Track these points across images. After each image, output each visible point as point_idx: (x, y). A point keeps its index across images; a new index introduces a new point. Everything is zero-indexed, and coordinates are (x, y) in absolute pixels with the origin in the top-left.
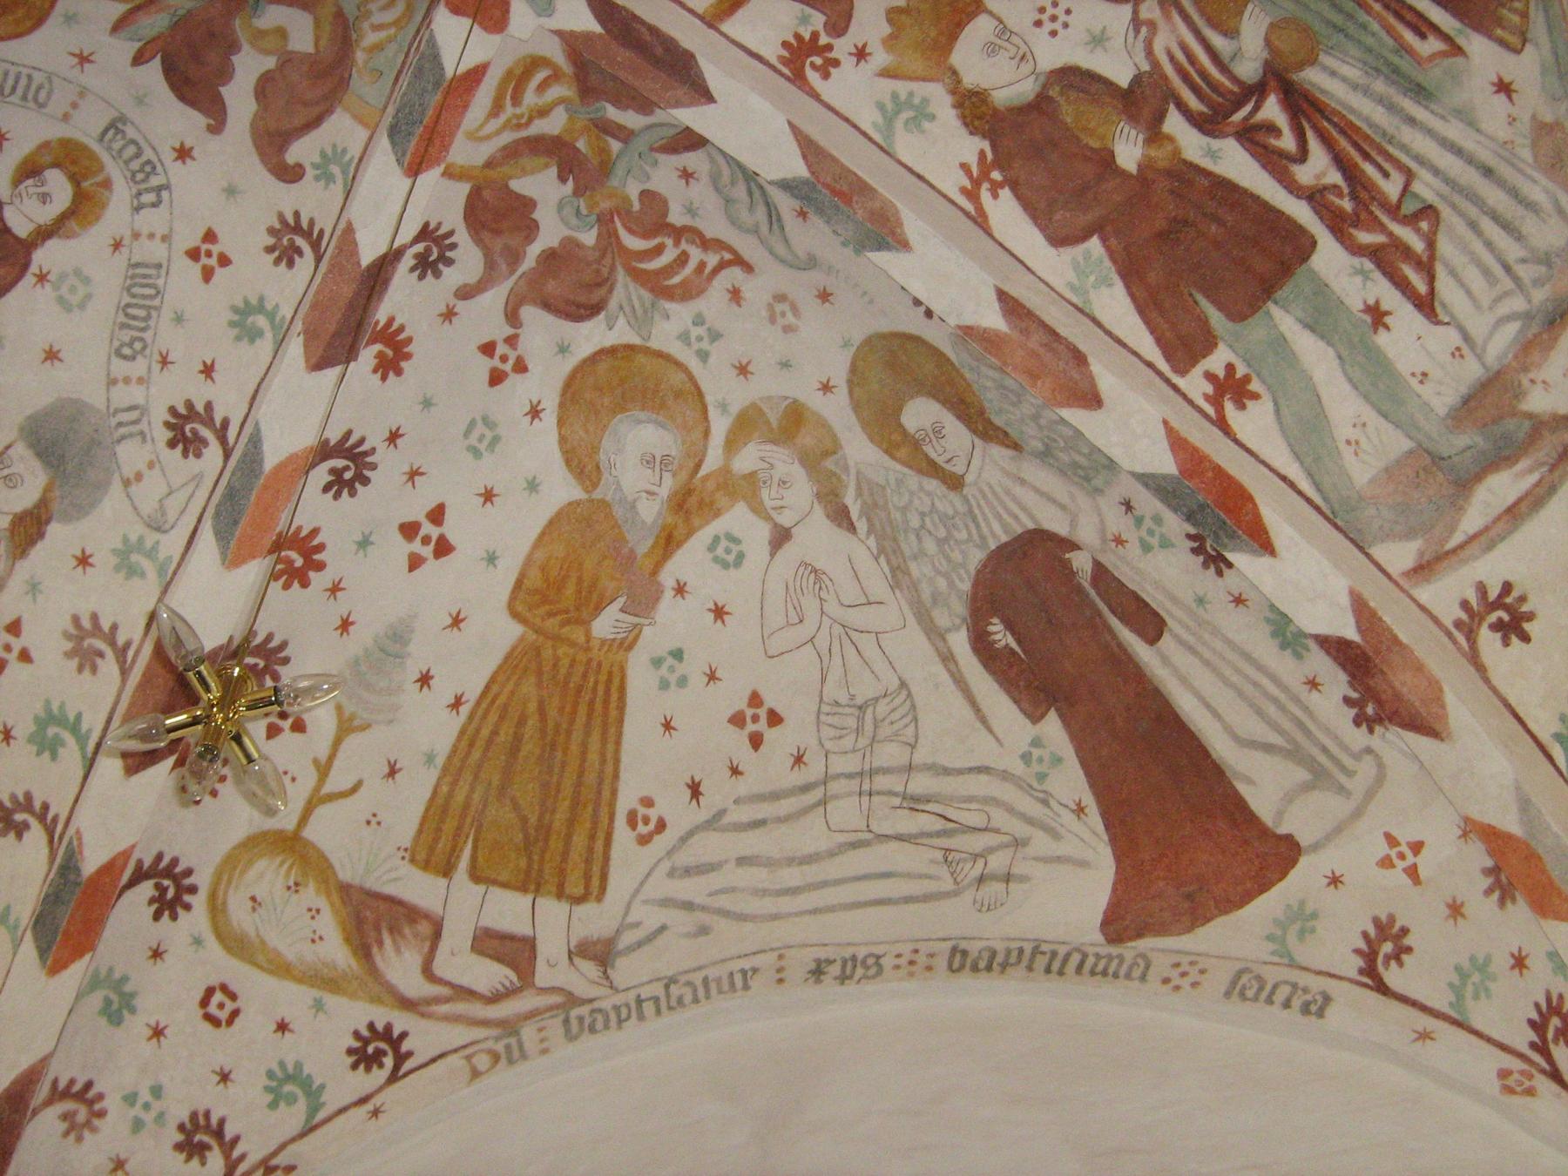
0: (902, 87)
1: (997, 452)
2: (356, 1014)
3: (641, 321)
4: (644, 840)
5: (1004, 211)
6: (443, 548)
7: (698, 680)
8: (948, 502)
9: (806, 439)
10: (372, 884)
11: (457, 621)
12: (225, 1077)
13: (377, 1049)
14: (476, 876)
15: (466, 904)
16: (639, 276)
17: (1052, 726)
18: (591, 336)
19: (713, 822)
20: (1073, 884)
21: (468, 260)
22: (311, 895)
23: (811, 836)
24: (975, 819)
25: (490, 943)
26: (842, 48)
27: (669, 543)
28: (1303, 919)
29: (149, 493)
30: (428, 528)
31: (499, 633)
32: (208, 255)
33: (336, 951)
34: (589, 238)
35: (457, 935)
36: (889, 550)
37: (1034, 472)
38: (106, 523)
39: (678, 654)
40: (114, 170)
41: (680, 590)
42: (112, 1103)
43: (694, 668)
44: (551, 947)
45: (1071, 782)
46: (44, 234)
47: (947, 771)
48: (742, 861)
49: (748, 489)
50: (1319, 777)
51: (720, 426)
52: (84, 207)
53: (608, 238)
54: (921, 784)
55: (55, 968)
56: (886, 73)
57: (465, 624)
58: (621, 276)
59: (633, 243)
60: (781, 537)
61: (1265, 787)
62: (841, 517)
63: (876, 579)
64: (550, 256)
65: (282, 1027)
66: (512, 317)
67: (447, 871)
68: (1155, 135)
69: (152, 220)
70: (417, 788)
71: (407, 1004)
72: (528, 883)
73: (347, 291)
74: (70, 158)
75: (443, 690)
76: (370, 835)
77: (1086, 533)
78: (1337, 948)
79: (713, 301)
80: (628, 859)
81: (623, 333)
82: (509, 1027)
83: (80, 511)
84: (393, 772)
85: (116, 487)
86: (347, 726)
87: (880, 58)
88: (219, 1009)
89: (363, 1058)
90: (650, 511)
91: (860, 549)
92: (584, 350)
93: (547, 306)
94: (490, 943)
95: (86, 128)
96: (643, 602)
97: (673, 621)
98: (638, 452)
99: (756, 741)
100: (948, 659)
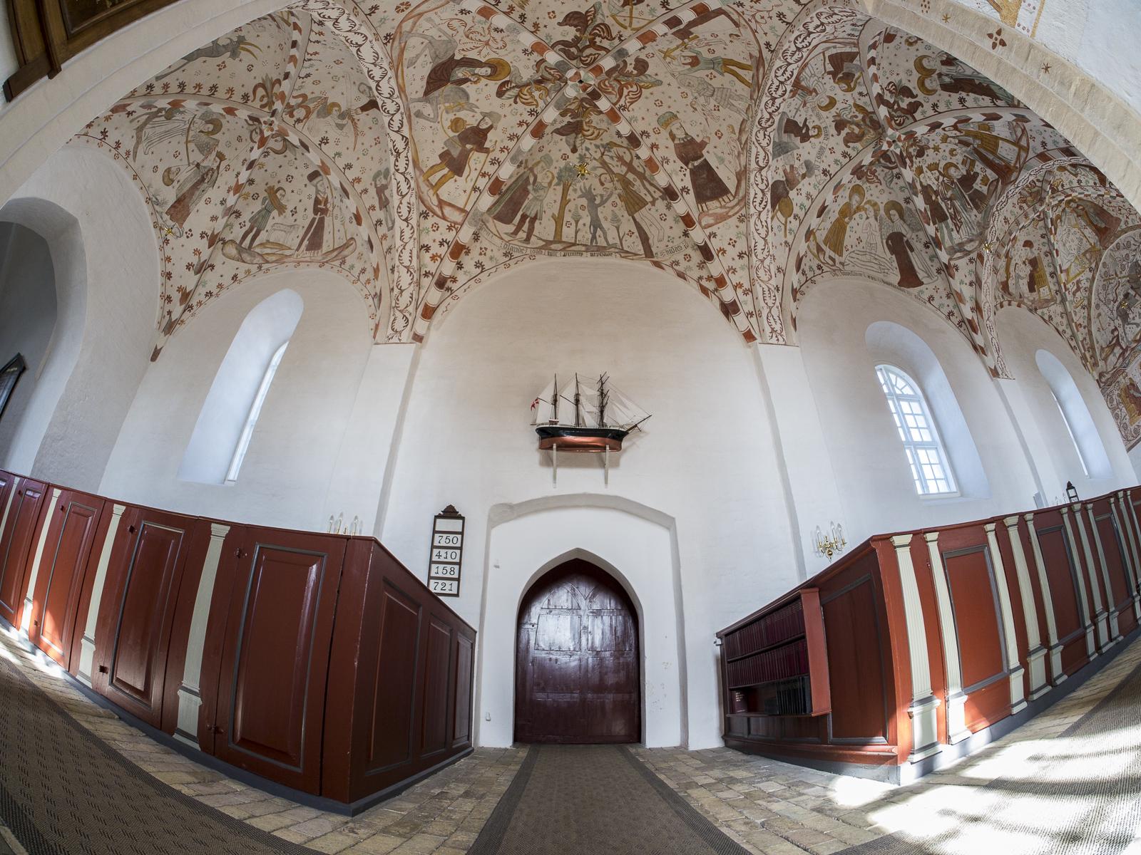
1: (902, 222)
8: (891, 224)
9: (876, 208)
13: (819, 267)
15: (829, 252)
17: (894, 256)
18: (858, 182)
20: (895, 277)
23: (864, 258)
25: (830, 257)
27: (855, 213)
28: (922, 292)
29: (819, 178)
31: (837, 215)
32: (832, 150)
36: (881, 225)
37: (905, 226)
38: (813, 180)
45: (895, 264)
46: (813, 136)
49: (865, 210)
50: (929, 276)
52: (818, 136)
60: (868, 218)
61: (921, 275)
62: (876, 219)
63: (878, 229)
70: (826, 232)
77: (908, 236)
78: (926, 297)
79: (873, 186)
80: (845, 253)
81: (861, 184)
83: (810, 177)
85: (814, 176)
90: (854, 207)
91: (877, 224)
94: (830, 257)
96: (850, 219)
97: (853, 223)
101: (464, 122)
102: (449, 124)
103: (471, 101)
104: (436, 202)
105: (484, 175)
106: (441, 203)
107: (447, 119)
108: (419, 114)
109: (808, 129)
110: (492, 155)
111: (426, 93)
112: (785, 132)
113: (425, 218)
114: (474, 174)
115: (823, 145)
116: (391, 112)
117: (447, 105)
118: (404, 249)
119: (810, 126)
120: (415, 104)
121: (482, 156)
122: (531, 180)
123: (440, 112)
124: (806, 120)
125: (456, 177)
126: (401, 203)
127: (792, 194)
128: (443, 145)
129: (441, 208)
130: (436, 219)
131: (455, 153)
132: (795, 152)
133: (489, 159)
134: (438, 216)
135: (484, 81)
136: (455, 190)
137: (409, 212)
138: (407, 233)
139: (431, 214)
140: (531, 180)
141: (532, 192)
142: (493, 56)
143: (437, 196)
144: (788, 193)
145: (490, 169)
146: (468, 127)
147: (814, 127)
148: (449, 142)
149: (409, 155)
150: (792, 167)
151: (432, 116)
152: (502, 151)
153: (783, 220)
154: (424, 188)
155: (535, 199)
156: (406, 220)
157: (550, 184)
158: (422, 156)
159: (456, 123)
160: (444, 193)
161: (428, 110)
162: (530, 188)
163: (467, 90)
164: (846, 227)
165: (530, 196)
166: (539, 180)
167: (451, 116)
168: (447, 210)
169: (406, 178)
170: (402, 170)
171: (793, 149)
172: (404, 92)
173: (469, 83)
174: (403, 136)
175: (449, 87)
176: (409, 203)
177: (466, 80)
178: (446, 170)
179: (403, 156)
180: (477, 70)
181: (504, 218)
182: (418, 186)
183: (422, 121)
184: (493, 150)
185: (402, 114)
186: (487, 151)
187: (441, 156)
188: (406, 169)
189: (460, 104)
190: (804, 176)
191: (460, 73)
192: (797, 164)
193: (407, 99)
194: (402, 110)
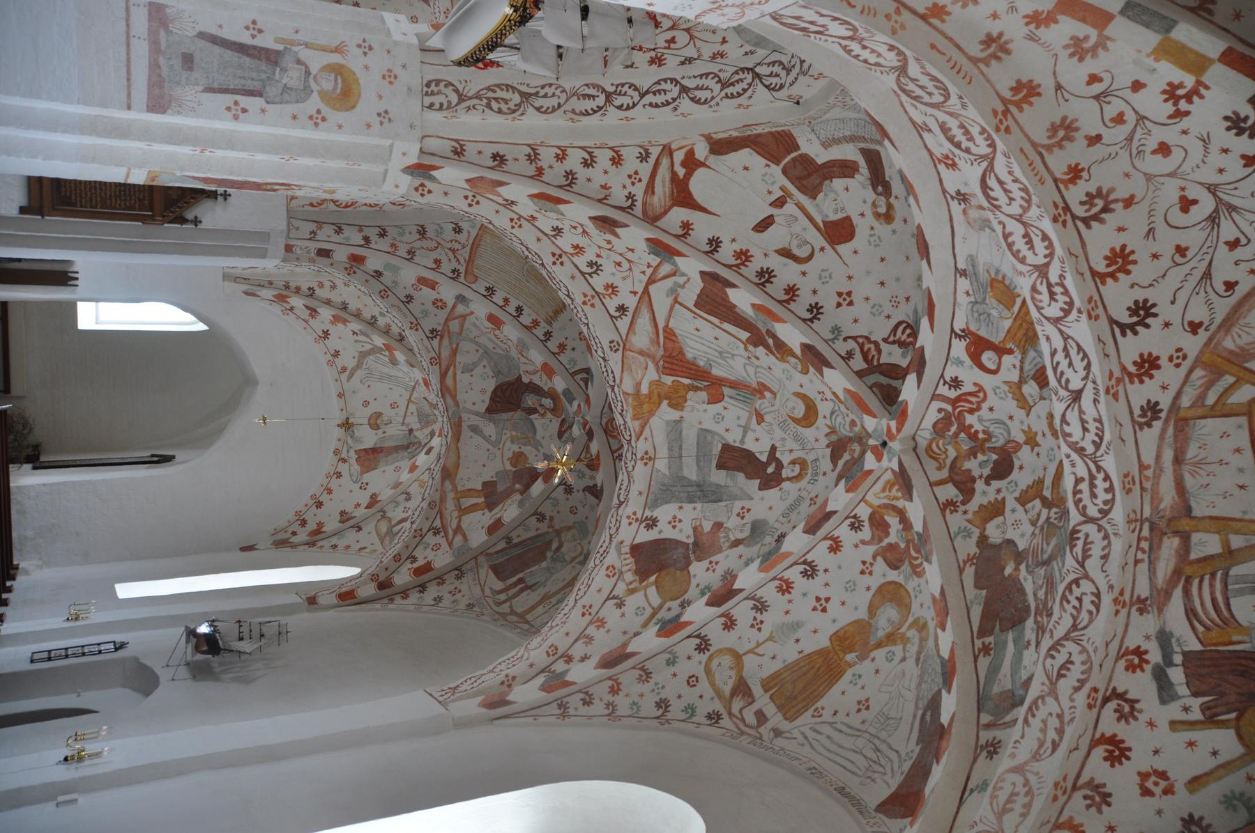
0: (969, 526)
2: (718, 706)
3: (907, 579)
4: (813, 716)
5: (970, 571)
6: (824, 610)
7: (859, 686)
10: (749, 681)
11: (815, 632)
12: (679, 697)
13: (714, 718)
14: (771, 698)
15: (762, 700)
16: (912, 565)
18: (893, 576)
19: (830, 724)
21: (866, 533)
22: (733, 673)
24: (883, 762)
26: (962, 508)
27: (879, 645)
30: (823, 601)
33: (727, 690)
34: (903, 545)
35: (755, 707)
36: (921, 677)
39: (860, 676)
40: (810, 471)
41: (873, 660)
42: (652, 681)
43: (860, 683)
44: (769, 725)
46: (788, 479)
47: (890, 748)
48: (828, 737)
49: (905, 641)
51: (910, 620)
52: (798, 478)
53: (907, 547)
54: (883, 747)
55: (658, 635)
56: (969, 521)
57: (817, 635)
58: (907, 562)
59: (913, 553)
62: (917, 660)
64: (890, 545)
65: (701, 697)
66: (874, 558)
67: (766, 691)
68: (1017, 569)
69: (810, 487)
71: (730, 714)
72: (780, 708)
73: (820, 516)
74: (802, 463)
75: (799, 647)
76: (758, 669)
80: (806, 718)
81: (900, 579)
82: (742, 733)
83: (749, 546)
84: (773, 658)
86: (771, 638)
87: (969, 516)
88: (692, 681)
89: (709, 717)
90: (880, 634)
91: (917, 672)
92: (890, 578)
93: (885, 560)
95: (810, 458)
96: (862, 658)
97: (866, 667)
98: (888, 615)
99: (859, 710)
100: (915, 717)
101: (527, 458)
104: (454, 525)
106: (459, 529)
107: (510, 449)
108: (475, 429)
109: (780, 466)
112: (720, 466)
113: (435, 534)
115: (804, 494)
119: (785, 459)
122: (555, 546)
124: (773, 448)
127: (698, 569)
129: (455, 533)
131: (501, 488)
132: (738, 505)
140: (555, 546)
141: (549, 560)
144: (689, 563)
147: (793, 462)
148: (502, 474)
150: (718, 526)
151: (493, 438)
153: (655, 600)
154: (450, 504)
155: (548, 569)
157: (574, 559)
158: (462, 473)
159: (518, 458)
161: (490, 430)
162: (549, 554)
163: (536, 423)
164: (840, 674)
165: (544, 564)
166: (564, 550)
167: (515, 448)
171: (736, 498)
172: (454, 397)
175: (519, 414)
177: (533, 411)
178: (482, 499)
181: (498, 571)
183: (478, 439)
187: (485, 484)
189: (527, 437)
190: (737, 543)
191: (530, 400)
192: (732, 522)
193: (458, 405)
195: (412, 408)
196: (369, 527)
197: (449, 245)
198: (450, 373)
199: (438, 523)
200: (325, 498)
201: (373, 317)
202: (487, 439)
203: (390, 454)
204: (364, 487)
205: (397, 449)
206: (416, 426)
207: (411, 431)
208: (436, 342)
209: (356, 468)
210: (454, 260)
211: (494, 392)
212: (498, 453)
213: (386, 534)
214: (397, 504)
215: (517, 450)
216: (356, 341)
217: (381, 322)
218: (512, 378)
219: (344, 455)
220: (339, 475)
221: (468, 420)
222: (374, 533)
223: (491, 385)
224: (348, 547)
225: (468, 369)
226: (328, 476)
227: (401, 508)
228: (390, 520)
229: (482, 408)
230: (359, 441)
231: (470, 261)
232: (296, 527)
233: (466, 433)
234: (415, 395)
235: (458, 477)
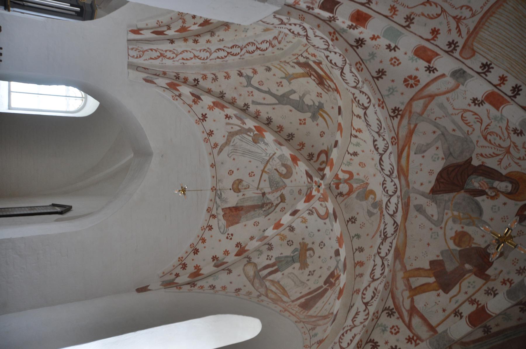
101: (471, 239)
102: (453, 235)
103: (486, 217)
104: (408, 307)
105: (473, 302)
106: (413, 310)
108: (420, 209)
110: (490, 284)
111: (434, 191)
113: (389, 315)
114: (462, 297)
116: (390, 193)
117: (456, 213)
118: (350, 330)
120: (419, 196)
121: (479, 282)
123: (446, 218)
125: (441, 291)
126: (369, 286)
128: (439, 254)
129: (411, 316)
130: (400, 323)
131: (450, 267)
133: (485, 288)
134: (404, 321)
135: (502, 198)
136: (433, 303)
137: (373, 298)
138: (361, 317)
139: (397, 315)
142: (514, 168)
143: (412, 301)
145: (481, 298)
146: (473, 245)
149: (395, 242)
151: (435, 218)
152: (504, 283)
156: (366, 304)
158: (410, 252)
159: (461, 237)
160: (422, 301)
161: (432, 209)
163: (482, 204)
167: (458, 228)
168: (416, 321)
169: (383, 264)
170: (383, 254)
172: (406, 177)
173: (484, 197)
174: (395, 222)
175: (462, 194)
176: (376, 289)
177: (481, 193)
179: (389, 240)
180: (496, 184)
182: (394, 279)
183: (421, 219)
184: (495, 280)
185: (398, 197)
186: (487, 278)
187: (432, 263)
188: (387, 255)
191: (476, 182)
193: (408, 185)
194: (398, 193)
195: (265, 176)
196: (237, 271)
197: (455, 13)
198: (405, 154)
199: (390, 304)
200: (200, 246)
201: (245, 105)
202: (429, 218)
203: (249, 211)
204: (230, 237)
205: (254, 208)
206: (267, 190)
207: (264, 194)
208: (396, 121)
209: (223, 222)
210: (454, 31)
211: (440, 174)
212: (441, 232)
213: (254, 277)
214: (261, 253)
215: (460, 229)
216: (227, 124)
217: (253, 109)
218: (460, 160)
219: (214, 212)
220: (210, 228)
221: (417, 200)
222: (243, 275)
223: (438, 166)
224: (224, 288)
225: (421, 151)
226: (203, 229)
227: (264, 256)
228: (255, 265)
229: (427, 188)
230: (225, 201)
231: (473, 34)
232: (179, 270)
233: (412, 212)
234: (269, 166)
235: (406, 256)
